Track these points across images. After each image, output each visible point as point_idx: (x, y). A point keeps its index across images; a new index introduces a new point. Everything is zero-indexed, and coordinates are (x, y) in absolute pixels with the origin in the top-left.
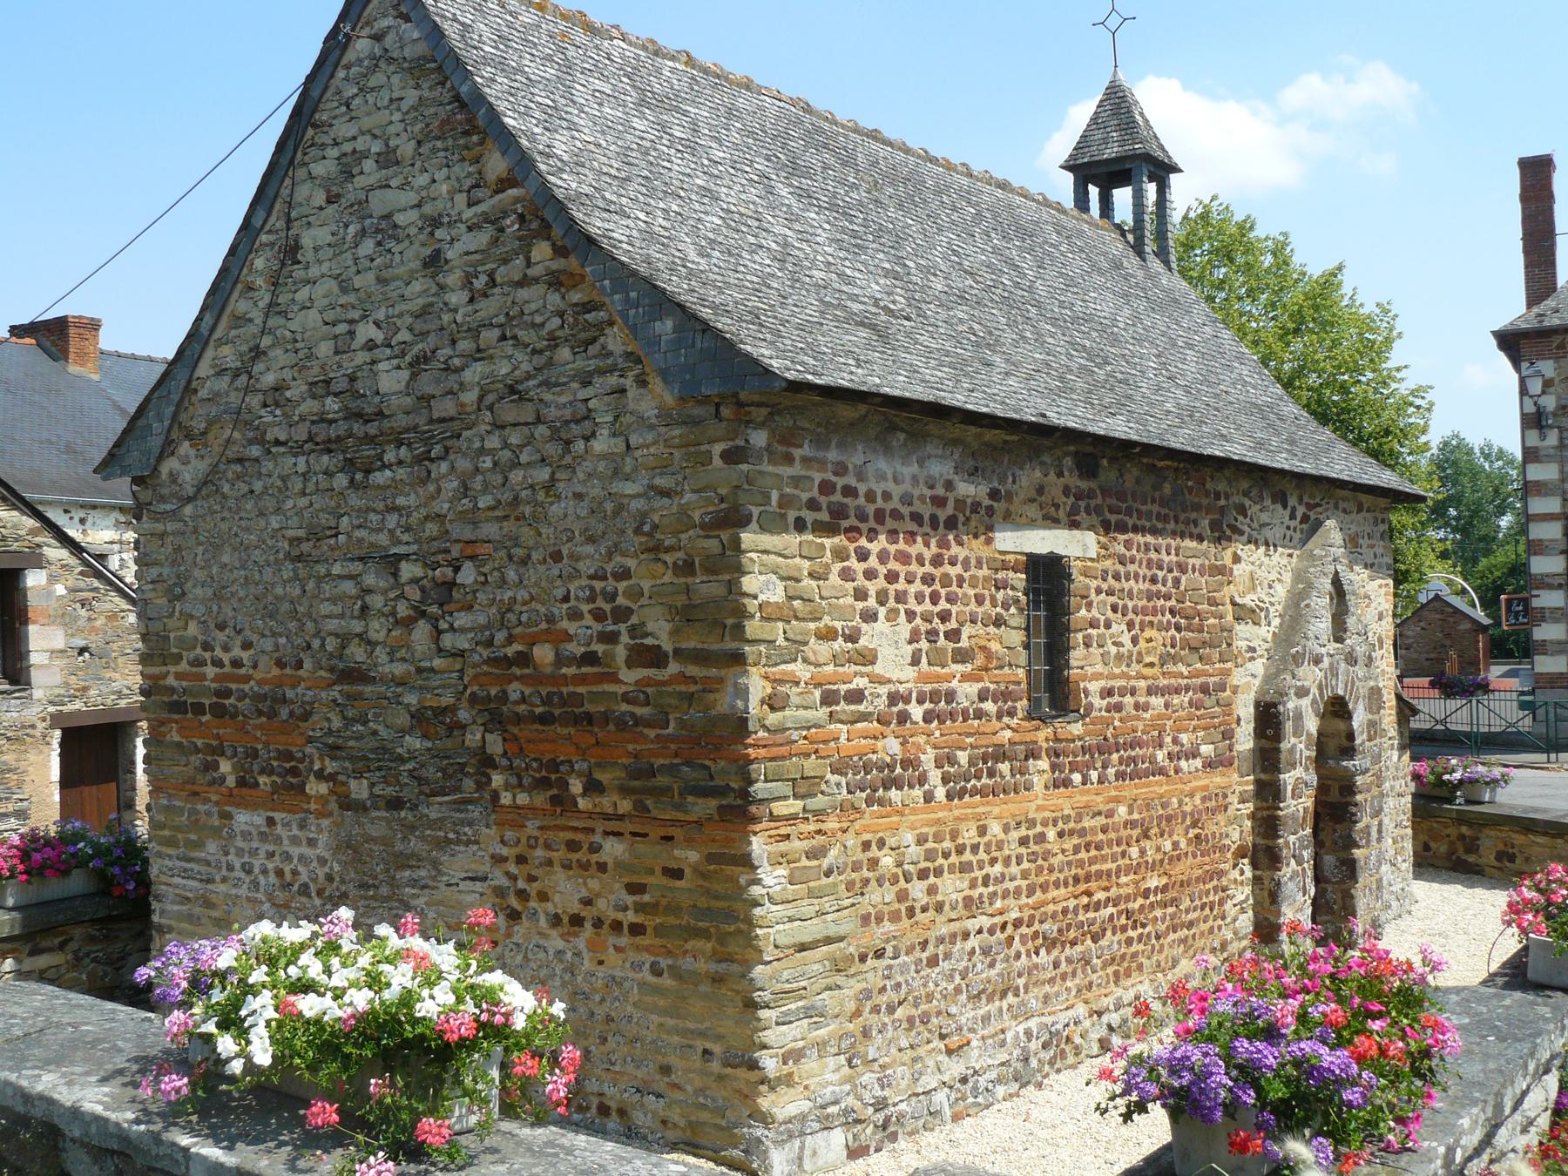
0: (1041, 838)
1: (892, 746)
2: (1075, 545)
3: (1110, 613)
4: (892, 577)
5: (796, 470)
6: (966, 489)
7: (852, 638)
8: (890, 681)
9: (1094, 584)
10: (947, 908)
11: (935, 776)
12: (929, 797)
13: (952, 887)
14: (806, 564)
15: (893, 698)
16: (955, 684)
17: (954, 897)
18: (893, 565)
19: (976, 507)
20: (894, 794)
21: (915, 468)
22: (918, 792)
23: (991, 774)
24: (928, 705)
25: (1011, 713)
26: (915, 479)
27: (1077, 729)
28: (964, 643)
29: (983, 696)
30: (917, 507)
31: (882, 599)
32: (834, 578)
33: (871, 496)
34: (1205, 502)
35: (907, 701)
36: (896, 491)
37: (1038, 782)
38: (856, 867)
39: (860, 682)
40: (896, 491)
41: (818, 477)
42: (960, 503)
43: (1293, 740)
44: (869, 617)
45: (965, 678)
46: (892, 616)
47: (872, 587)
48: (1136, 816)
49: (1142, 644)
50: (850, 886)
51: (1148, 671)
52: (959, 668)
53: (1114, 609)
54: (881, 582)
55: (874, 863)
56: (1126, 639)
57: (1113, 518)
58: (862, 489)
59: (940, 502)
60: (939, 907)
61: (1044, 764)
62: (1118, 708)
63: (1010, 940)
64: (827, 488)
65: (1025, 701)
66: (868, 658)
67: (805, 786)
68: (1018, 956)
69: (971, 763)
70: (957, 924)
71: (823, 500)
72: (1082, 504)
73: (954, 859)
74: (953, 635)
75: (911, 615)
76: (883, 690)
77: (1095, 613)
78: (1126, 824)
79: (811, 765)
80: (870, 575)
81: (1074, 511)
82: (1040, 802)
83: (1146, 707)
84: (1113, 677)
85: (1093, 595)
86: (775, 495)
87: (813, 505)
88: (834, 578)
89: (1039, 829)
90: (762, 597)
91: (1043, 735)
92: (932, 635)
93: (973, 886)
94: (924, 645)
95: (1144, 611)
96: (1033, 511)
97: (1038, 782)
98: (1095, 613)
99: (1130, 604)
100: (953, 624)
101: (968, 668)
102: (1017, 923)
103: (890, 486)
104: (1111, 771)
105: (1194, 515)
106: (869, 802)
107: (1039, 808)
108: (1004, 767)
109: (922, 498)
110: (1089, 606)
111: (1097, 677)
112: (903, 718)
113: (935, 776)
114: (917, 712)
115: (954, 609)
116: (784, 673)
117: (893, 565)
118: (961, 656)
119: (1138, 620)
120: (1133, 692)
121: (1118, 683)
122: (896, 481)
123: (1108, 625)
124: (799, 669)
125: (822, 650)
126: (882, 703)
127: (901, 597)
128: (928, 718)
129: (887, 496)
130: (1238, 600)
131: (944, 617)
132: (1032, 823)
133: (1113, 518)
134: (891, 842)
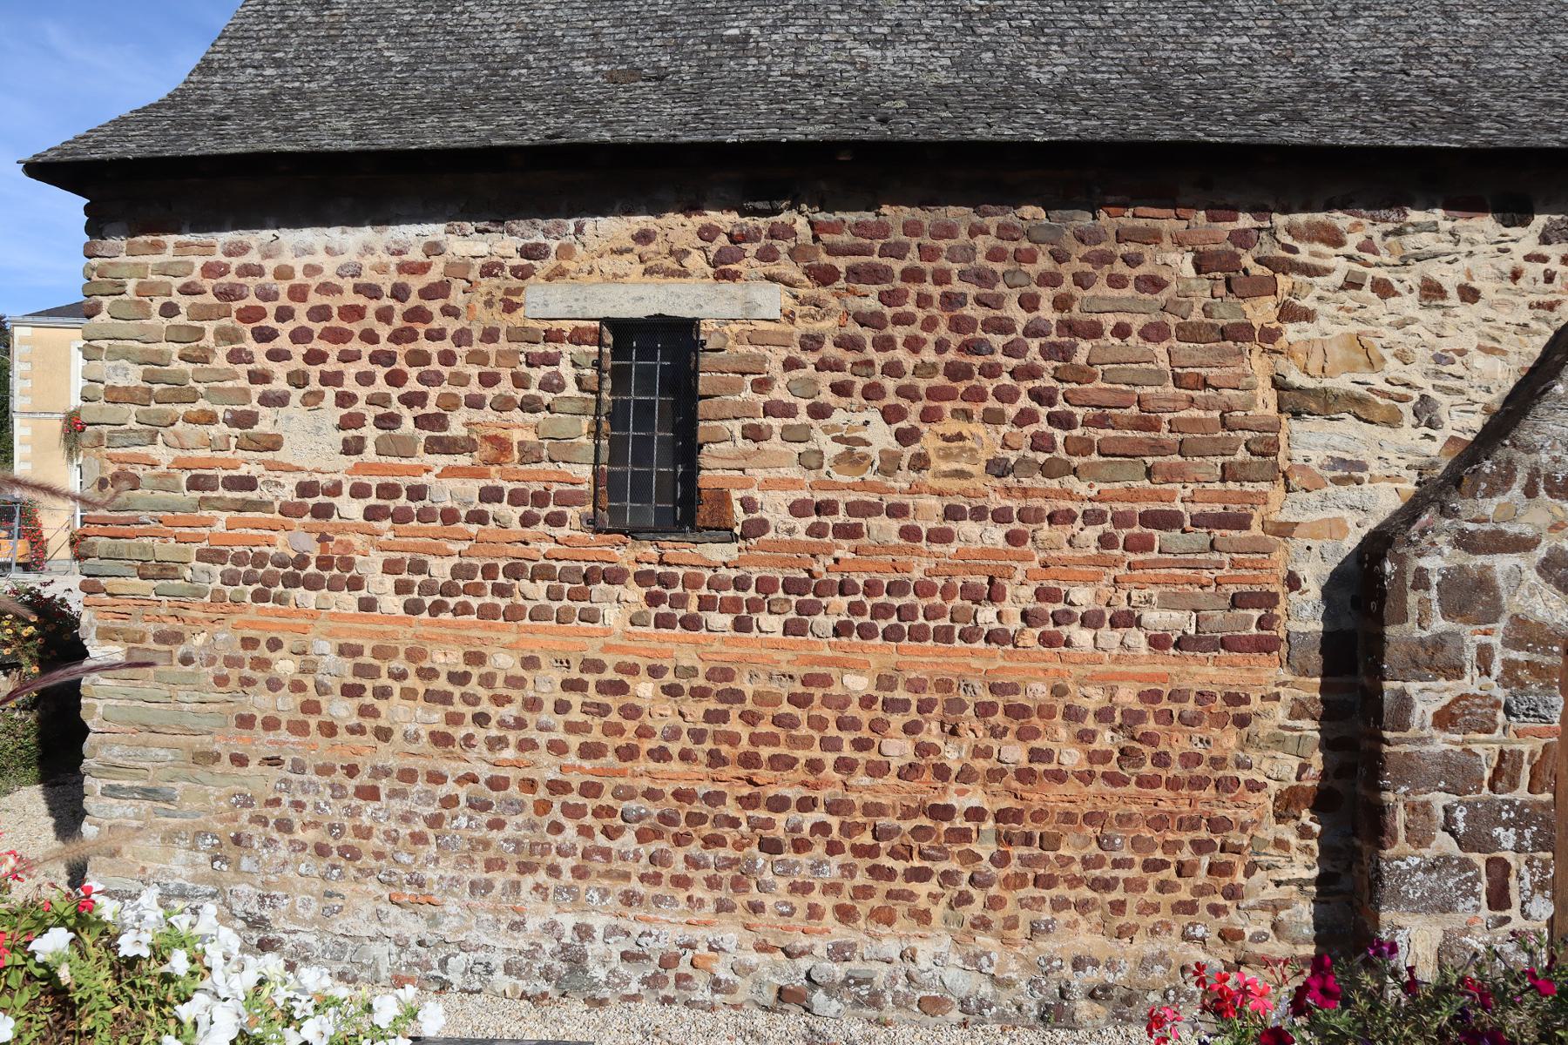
0: (619, 688)
1: (294, 540)
5: (167, 256)
7: (245, 420)
8: (299, 469)
10: (397, 736)
11: (381, 585)
12: (368, 605)
13: (410, 717)
14: (176, 348)
15: (305, 489)
16: (425, 479)
17: (411, 728)
19: (489, 271)
20: (299, 593)
22: (348, 600)
23: (500, 591)
24: (373, 500)
30: (368, 277)
31: (298, 379)
32: (220, 361)
33: (283, 273)
35: (335, 490)
39: (254, 470)
41: (199, 262)
42: (459, 269)
43: (1439, 624)
45: (449, 472)
46: (310, 399)
47: (280, 370)
48: (900, 693)
49: (929, 442)
51: (955, 484)
52: (443, 460)
54: (297, 363)
56: (881, 436)
58: (270, 265)
60: (384, 734)
63: (543, 807)
64: (210, 270)
65: (589, 508)
66: (274, 443)
68: (557, 828)
69: (457, 571)
70: (422, 761)
71: (208, 284)
73: (412, 681)
75: (344, 399)
76: (290, 482)
78: (867, 702)
79: (165, 550)
80: (277, 356)
82: (611, 640)
84: (835, 486)
85: (774, 368)
86: (131, 285)
87: (187, 290)
88: (220, 361)
89: (610, 675)
90: (109, 382)
92: (388, 422)
93: (455, 719)
94: (370, 432)
95: (933, 393)
97: (613, 616)
98: (779, 393)
100: (431, 408)
101: (463, 460)
102: (557, 787)
103: (320, 258)
104: (824, 622)
105: (1131, 248)
106: (259, 597)
107: (607, 648)
109: (382, 269)
110: (762, 385)
112: (323, 512)
115: (433, 393)
116: (135, 455)
119: (916, 408)
120: (897, 511)
121: (843, 498)
122: (329, 251)
126: (288, 494)
128: (371, 514)
129: (312, 270)
131: (410, 400)
132: (599, 667)
133: (841, 263)
134: (288, 641)
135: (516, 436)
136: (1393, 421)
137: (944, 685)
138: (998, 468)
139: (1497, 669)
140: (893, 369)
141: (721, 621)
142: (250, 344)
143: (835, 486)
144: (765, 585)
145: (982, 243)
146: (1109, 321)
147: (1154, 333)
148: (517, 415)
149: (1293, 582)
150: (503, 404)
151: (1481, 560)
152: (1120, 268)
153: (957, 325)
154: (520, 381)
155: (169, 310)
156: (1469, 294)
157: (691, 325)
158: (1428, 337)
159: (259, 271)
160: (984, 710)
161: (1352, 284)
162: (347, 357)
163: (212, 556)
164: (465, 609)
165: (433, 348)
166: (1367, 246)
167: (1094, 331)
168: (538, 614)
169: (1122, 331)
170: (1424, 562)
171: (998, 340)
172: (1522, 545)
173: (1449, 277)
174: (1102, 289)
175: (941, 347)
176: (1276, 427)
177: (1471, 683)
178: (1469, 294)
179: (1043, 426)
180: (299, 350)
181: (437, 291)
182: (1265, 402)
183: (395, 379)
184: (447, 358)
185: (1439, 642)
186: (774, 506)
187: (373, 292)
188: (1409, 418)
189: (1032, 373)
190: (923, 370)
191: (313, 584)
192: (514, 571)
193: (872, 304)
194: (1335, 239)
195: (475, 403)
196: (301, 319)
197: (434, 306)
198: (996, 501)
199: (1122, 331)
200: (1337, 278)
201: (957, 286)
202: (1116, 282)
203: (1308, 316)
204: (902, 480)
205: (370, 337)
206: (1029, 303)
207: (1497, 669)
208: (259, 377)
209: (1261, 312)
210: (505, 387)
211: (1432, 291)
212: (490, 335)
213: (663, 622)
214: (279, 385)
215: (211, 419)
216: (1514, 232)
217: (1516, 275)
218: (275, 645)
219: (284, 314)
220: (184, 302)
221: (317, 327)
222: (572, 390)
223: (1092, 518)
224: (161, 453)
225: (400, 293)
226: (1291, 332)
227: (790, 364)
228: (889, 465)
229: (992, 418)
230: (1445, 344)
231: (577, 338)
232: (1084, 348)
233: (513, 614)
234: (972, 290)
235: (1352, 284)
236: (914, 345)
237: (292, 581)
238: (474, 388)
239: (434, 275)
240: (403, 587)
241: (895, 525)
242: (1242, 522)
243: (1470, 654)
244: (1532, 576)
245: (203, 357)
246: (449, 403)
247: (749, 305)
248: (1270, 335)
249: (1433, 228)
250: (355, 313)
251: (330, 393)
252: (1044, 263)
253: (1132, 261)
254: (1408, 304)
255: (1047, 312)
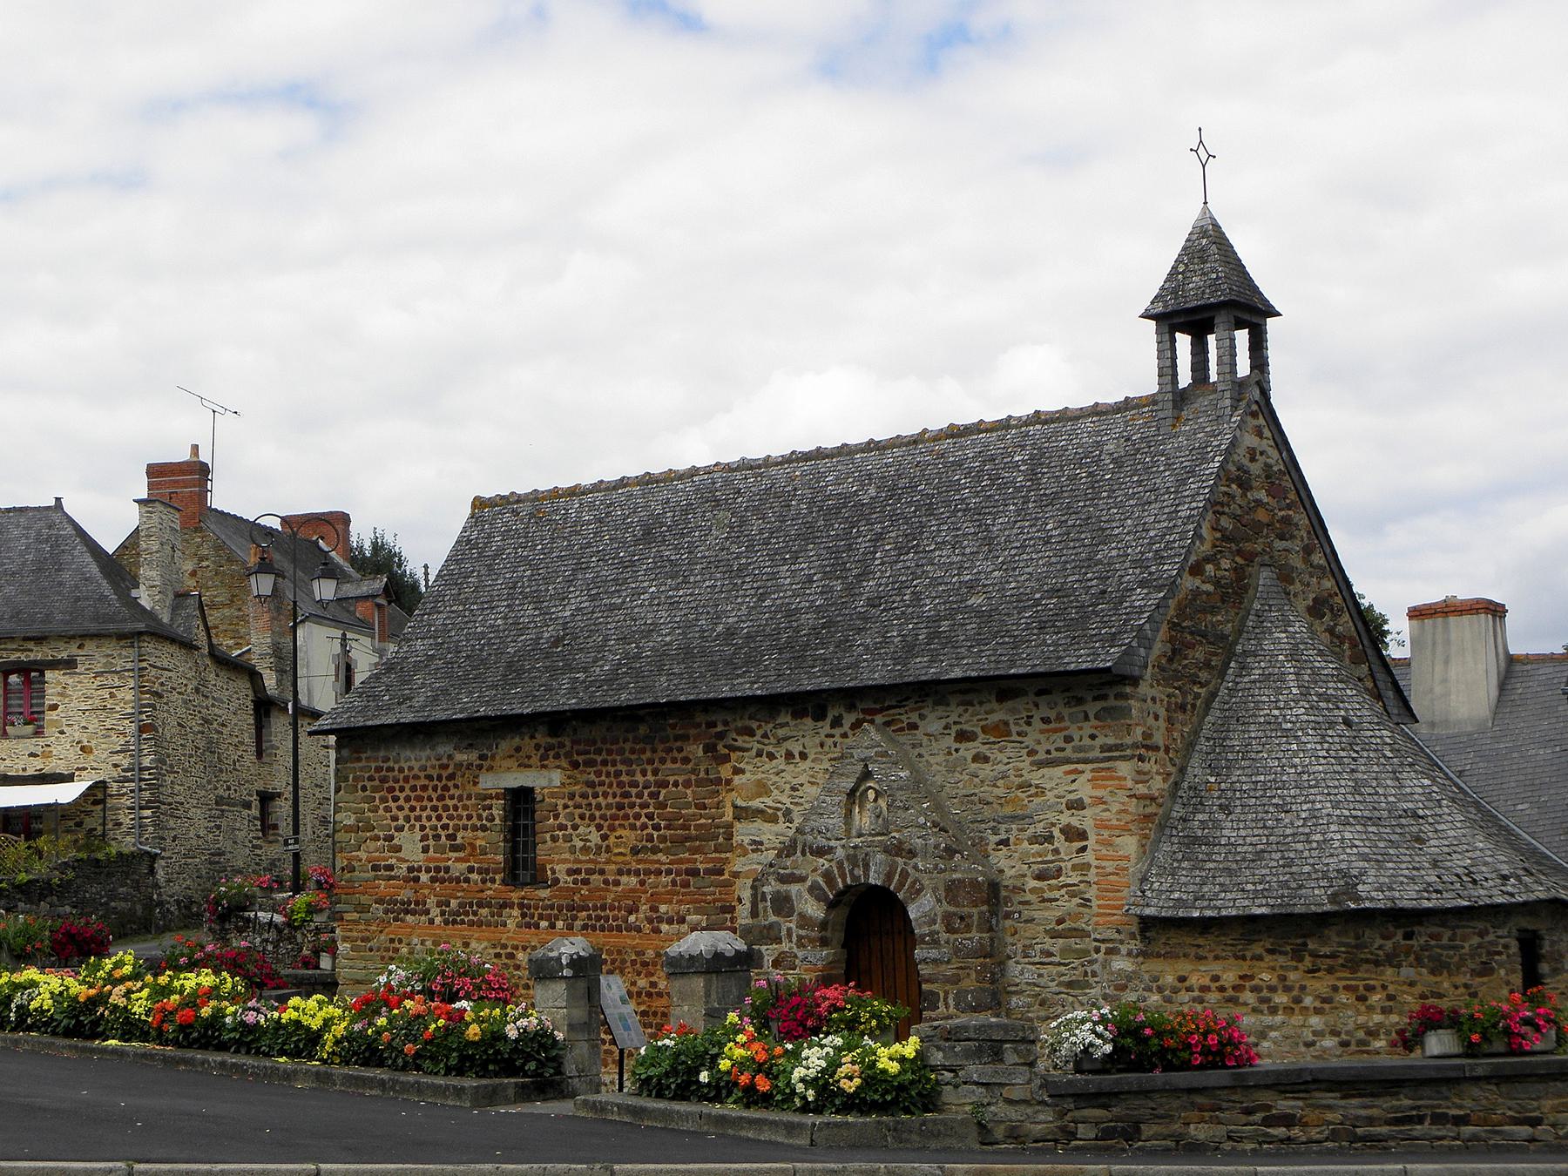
0: (511, 956)
1: (406, 894)
2: (546, 780)
3: (577, 820)
4: (413, 809)
6: (460, 757)
7: (390, 838)
9: (560, 802)
11: (435, 911)
12: (431, 922)
15: (411, 869)
18: (413, 803)
20: (409, 918)
21: (428, 752)
23: (475, 913)
25: (493, 881)
26: (429, 758)
27: (544, 893)
28: (459, 841)
29: (471, 870)
30: (430, 771)
31: (407, 819)
32: (381, 812)
33: (401, 770)
34: (692, 732)
36: (416, 765)
37: (511, 924)
38: (387, 950)
39: (393, 861)
40: (416, 765)
42: (459, 766)
43: (773, 918)
44: (400, 829)
45: (457, 860)
47: (401, 815)
49: (612, 840)
50: (383, 958)
51: (620, 859)
52: (454, 855)
53: (582, 817)
54: (407, 812)
55: (396, 950)
56: (595, 838)
57: (580, 759)
59: (445, 767)
61: (516, 912)
62: (586, 882)
66: (398, 849)
67: (363, 909)
69: (461, 905)
72: (551, 753)
74: (452, 837)
75: (423, 828)
76: (404, 866)
77: (562, 820)
79: (364, 899)
80: (400, 808)
81: (543, 758)
83: (617, 883)
84: (580, 862)
85: (560, 808)
87: (371, 779)
88: (381, 812)
91: (515, 896)
92: (437, 837)
94: (431, 842)
95: (614, 817)
96: (512, 763)
97: (511, 924)
98: (562, 820)
99: (598, 814)
101: (462, 854)
103: (413, 763)
104: (578, 923)
105: (679, 744)
106: (396, 919)
108: (484, 911)
109: (433, 767)
110: (556, 817)
111: (565, 861)
112: (417, 879)
113: (435, 911)
114: (424, 877)
117: (413, 803)
118: (454, 848)
120: (602, 872)
123: (575, 827)
124: (363, 855)
125: (371, 845)
127: (418, 819)
129: (410, 768)
130: (740, 803)
132: (504, 946)
133: (580, 759)
135: (478, 843)
136: (774, 820)
137: (619, 952)
138: (635, 851)
139: (794, 939)
140: (599, 807)
141: (544, 924)
142: (391, 804)
143: (580, 862)
144: (560, 909)
145: (628, 746)
146: (672, 779)
147: (687, 784)
148: (480, 834)
149: (740, 900)
150: (475, 828)
151: (785, 887)
152: (675, 754)
153: (621, 785)
154: (480, 817)
155: (364, 789)
156: (803, 756)
157: (531, 790)
158: (789, 778)
159: (392, 769)
160: (634, 962)
161: (759, 754)
162: (423, 809)
163: (380, 901)
164: (463, 922)
165: (450, 803)
166: (765, 736)
167: (665, 784)
168: (489, 925)
169: (676, 784)
170: (766, 889)
171: (634, 791)
172: (802, 879)
173: (796, 749)
174: (669, 765)
175: (614, 796)
176: (730, 826)
177: (785, 946)
178: (803, 756)
179: (650, 830)
180: (407, 806)
181: (451, 777)
182: (729, 815)
183: (439, 818)
184: (456, 808)
185: (771, 926)
186: (561, 869)
187: (430, 778)
188: (781, 819)
189: (644, 806)
190: (609, 806)
191: (414, 913)
192: (480, 905)
193: (592, 777)
194: (751, 733)
195: (465, 828)
196: (408, 792)
197: (450, 784)
198: (634, 866)
199: (676, 784)
200: (754, 752)
201: (620, 767)
202: (674, 761)
203: (742, 771)
204: (603, 857)
205: (430, 799)
206: (644, 773)
207: (794, 939)
208: (395, 819)
209: (725, 771)
210: (475, 820)
211: (789, 755)
212: (469, 797)
213: (528, 926)
214: (401, 822)
215: (377, 838)
216: (820, 724)
217: (822, 745)
218: (400, 941)
219: (402, 790)
220: (368, 784)
221: (413, 795)
222: (497, 821)
223: (669, 872)
224: (363, 855)
225: (440, 778)
226: (737, 780)
227: (566, 807)
228: (599, 847)
229: (633, 827)
230: (795, 781)
231: (497, 797)
232: (663, 792)
233: (480, 924)
234: (623, 768)
235: (759, 754)
236: (605, 795)
237: (407, 912)
238: (465, 821)
239: (450, 770)
240: (443, 913)
241: (601, 878)
242: (721, 872)
243: (784, 932)
244: (807, 896)
245: (376, 810)
246: (457, 828)
247: (551, 780)
248: (729, 782)
249: (787, 724)
250: (424, 788)
251: (418, 825)
252: (648, 754)
253: (680, 750)
254: (780, 762)
255: (650, 777)
